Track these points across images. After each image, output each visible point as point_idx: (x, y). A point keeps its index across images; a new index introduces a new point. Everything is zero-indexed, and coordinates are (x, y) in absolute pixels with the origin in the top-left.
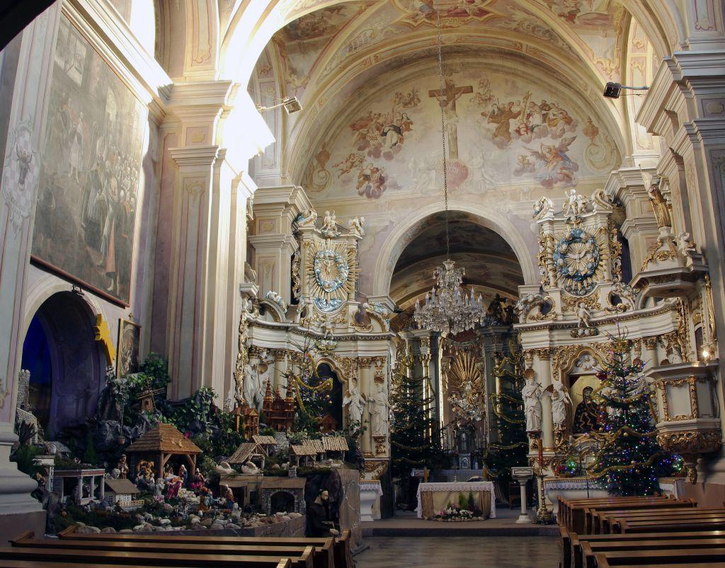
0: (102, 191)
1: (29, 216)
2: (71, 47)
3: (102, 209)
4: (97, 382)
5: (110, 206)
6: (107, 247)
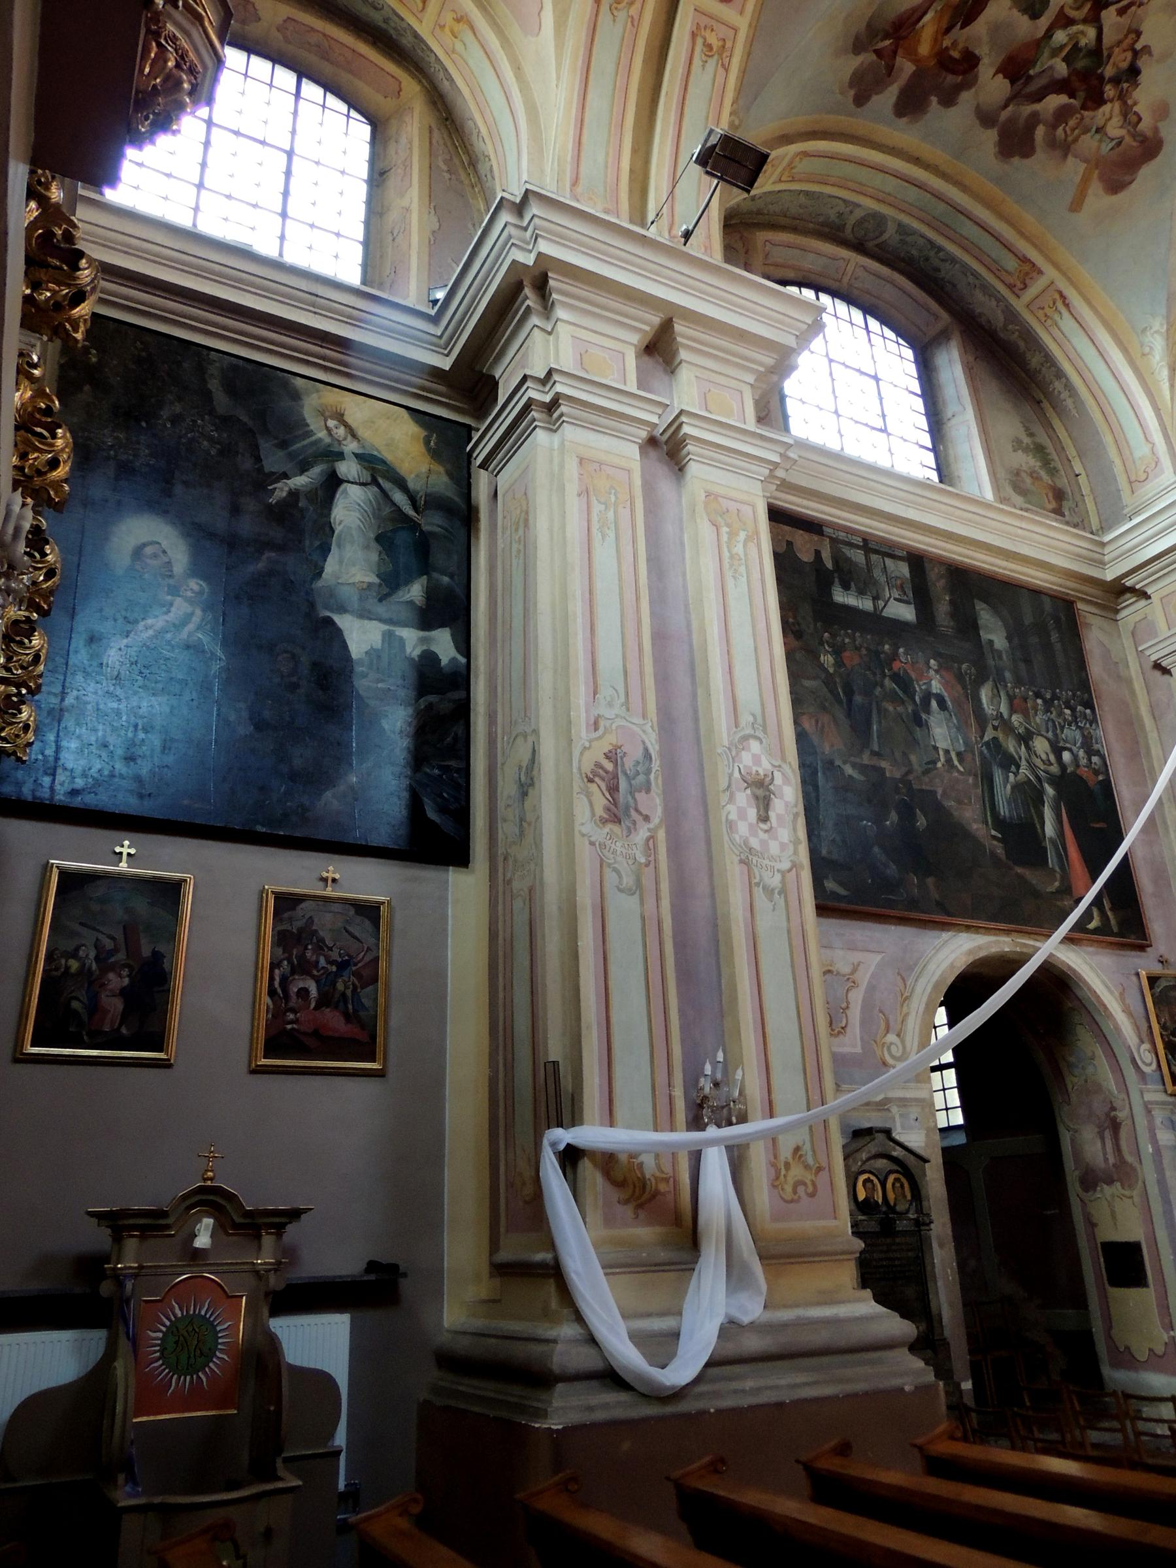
0: (1018, 767)
1: (795, 866)
2: (877, 573)
3: (1030, 794)
4: (1123, 1096)
5: (1046, 786)
6: (1063, 858)
